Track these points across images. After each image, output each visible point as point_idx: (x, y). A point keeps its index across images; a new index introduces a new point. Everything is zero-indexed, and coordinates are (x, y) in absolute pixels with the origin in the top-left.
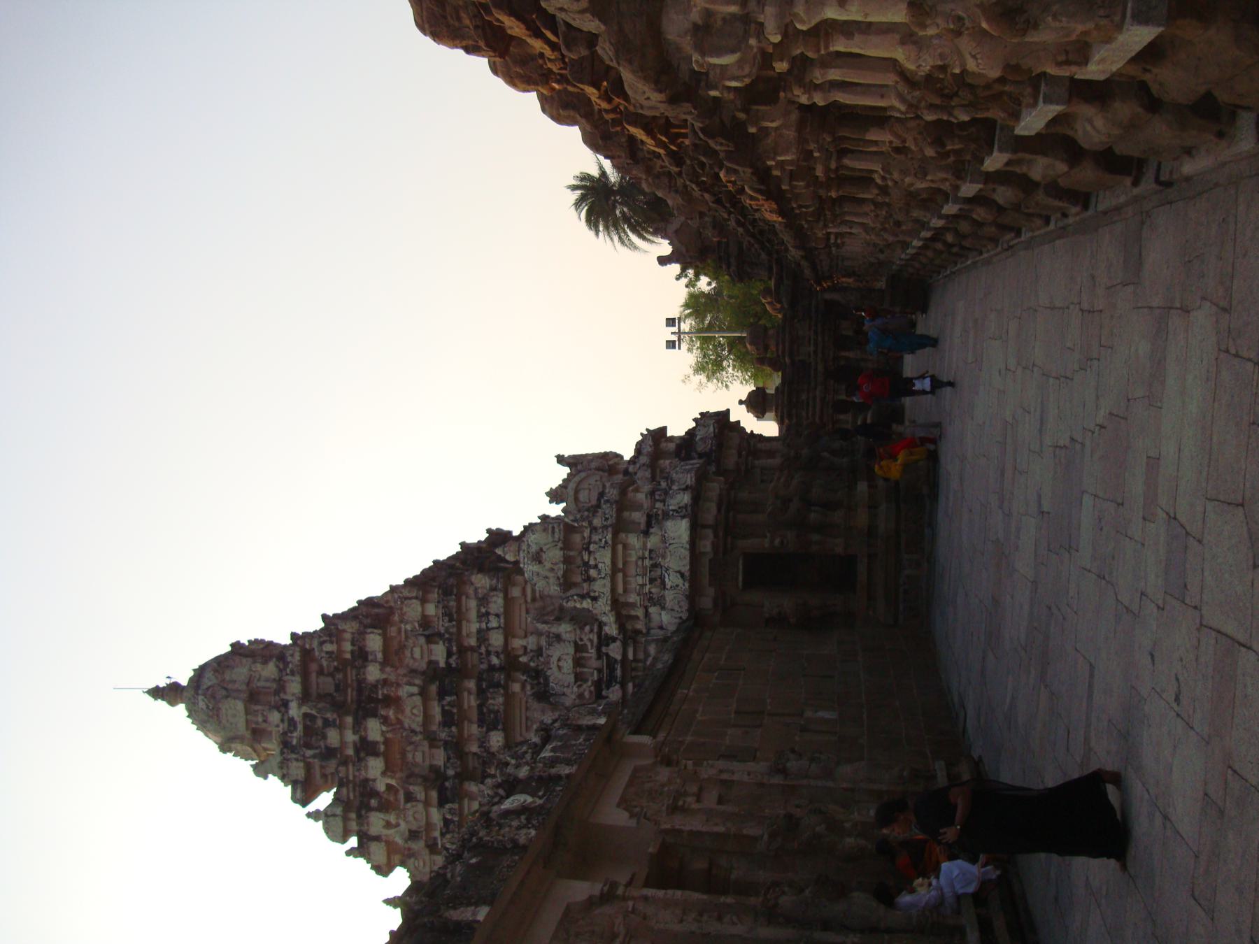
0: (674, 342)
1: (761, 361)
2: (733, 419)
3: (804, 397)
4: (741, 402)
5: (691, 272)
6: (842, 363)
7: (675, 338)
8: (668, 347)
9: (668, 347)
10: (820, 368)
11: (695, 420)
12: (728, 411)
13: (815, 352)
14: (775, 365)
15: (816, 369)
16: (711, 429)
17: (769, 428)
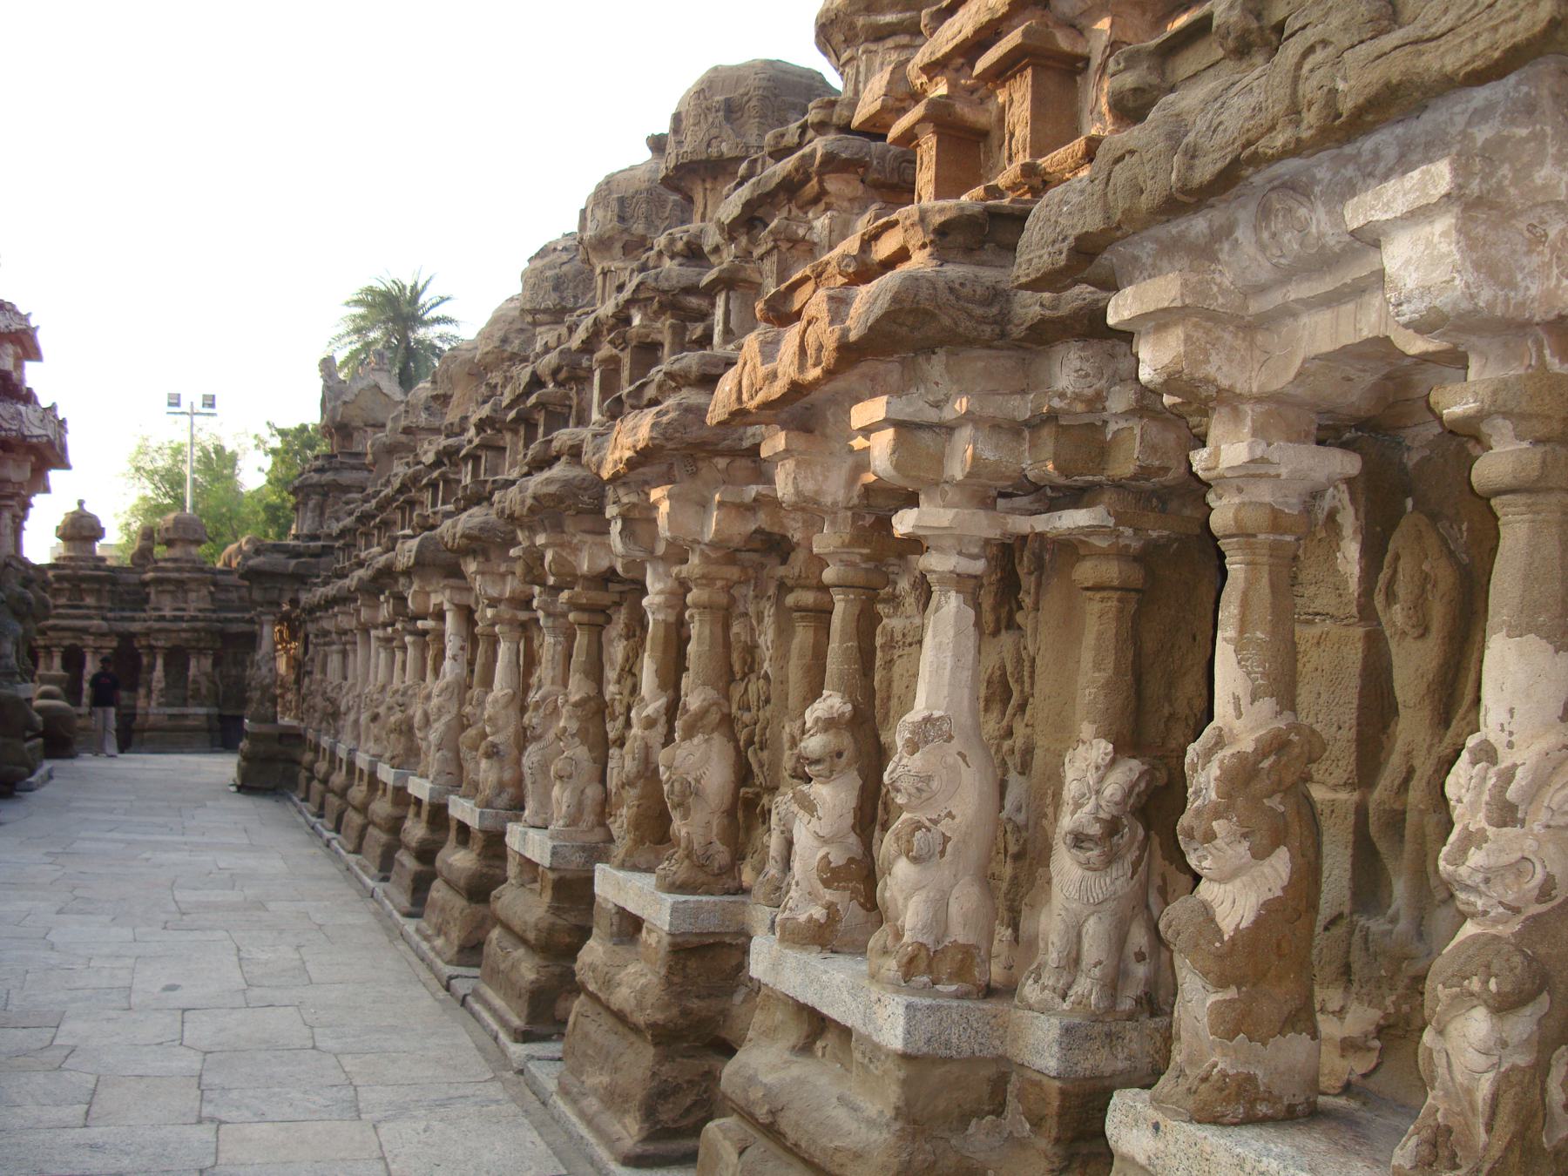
0: (178, 405)
1: (148, 534)
2: (54, 476)
3: (90, 601)
4: (81, 503)
5: (277, 443)
6: (145, 660)
7: (185, 407)
8: (171, 396)
9: (171, 396)
10: (136, 627)
11: (53, 408)
12: (67, 466)
13: (163, 618)
14: (143, 555)
15: (133, 619)
16: (37, 432)
17: (40, 543)
